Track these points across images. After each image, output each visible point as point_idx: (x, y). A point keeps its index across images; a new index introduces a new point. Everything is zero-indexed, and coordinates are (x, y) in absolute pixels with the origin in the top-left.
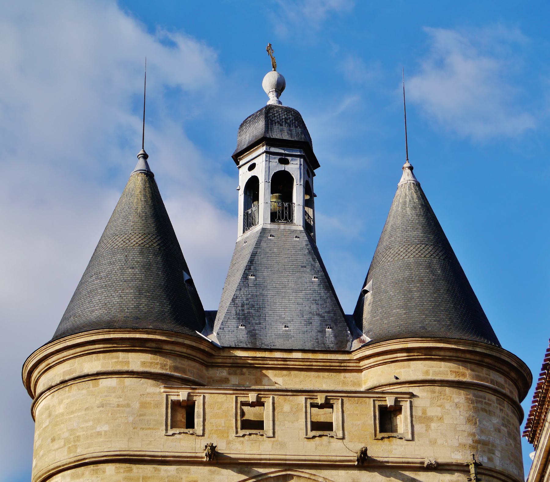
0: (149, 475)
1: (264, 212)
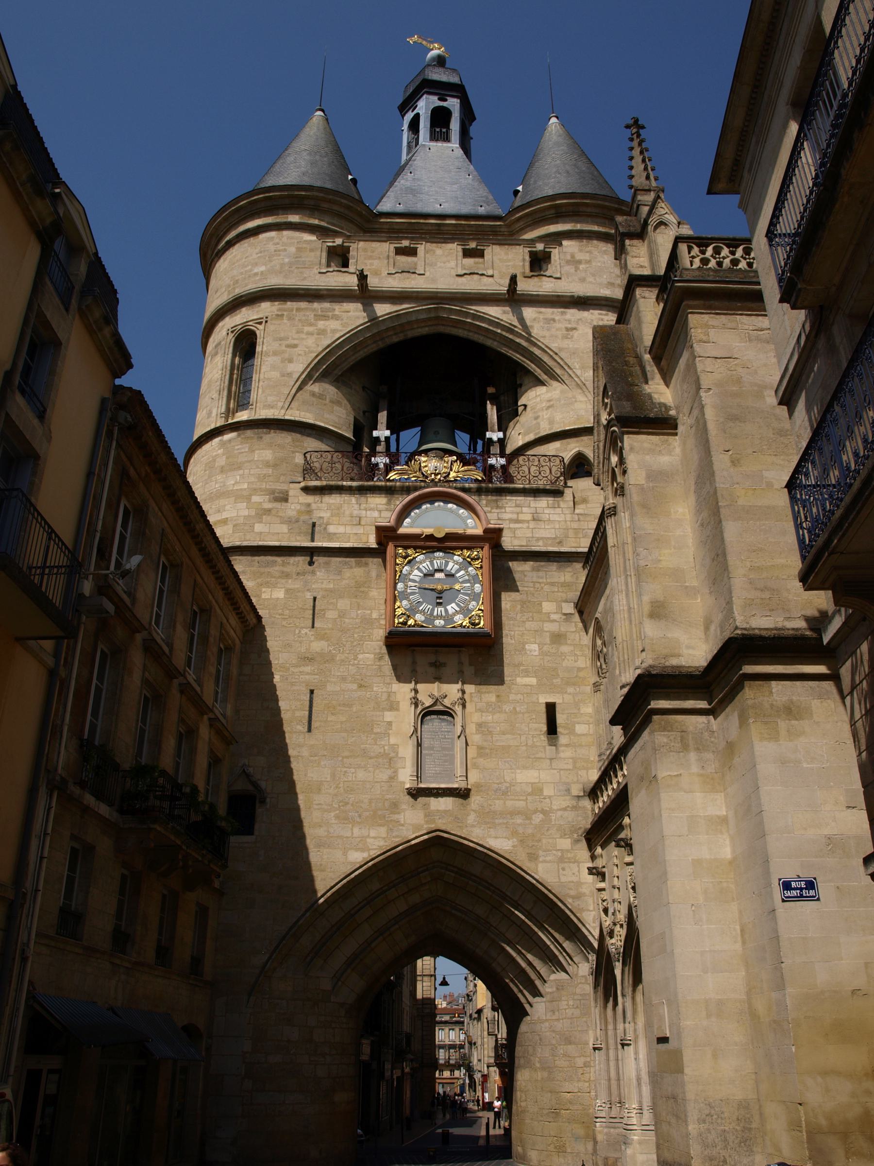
1: (425, 134)
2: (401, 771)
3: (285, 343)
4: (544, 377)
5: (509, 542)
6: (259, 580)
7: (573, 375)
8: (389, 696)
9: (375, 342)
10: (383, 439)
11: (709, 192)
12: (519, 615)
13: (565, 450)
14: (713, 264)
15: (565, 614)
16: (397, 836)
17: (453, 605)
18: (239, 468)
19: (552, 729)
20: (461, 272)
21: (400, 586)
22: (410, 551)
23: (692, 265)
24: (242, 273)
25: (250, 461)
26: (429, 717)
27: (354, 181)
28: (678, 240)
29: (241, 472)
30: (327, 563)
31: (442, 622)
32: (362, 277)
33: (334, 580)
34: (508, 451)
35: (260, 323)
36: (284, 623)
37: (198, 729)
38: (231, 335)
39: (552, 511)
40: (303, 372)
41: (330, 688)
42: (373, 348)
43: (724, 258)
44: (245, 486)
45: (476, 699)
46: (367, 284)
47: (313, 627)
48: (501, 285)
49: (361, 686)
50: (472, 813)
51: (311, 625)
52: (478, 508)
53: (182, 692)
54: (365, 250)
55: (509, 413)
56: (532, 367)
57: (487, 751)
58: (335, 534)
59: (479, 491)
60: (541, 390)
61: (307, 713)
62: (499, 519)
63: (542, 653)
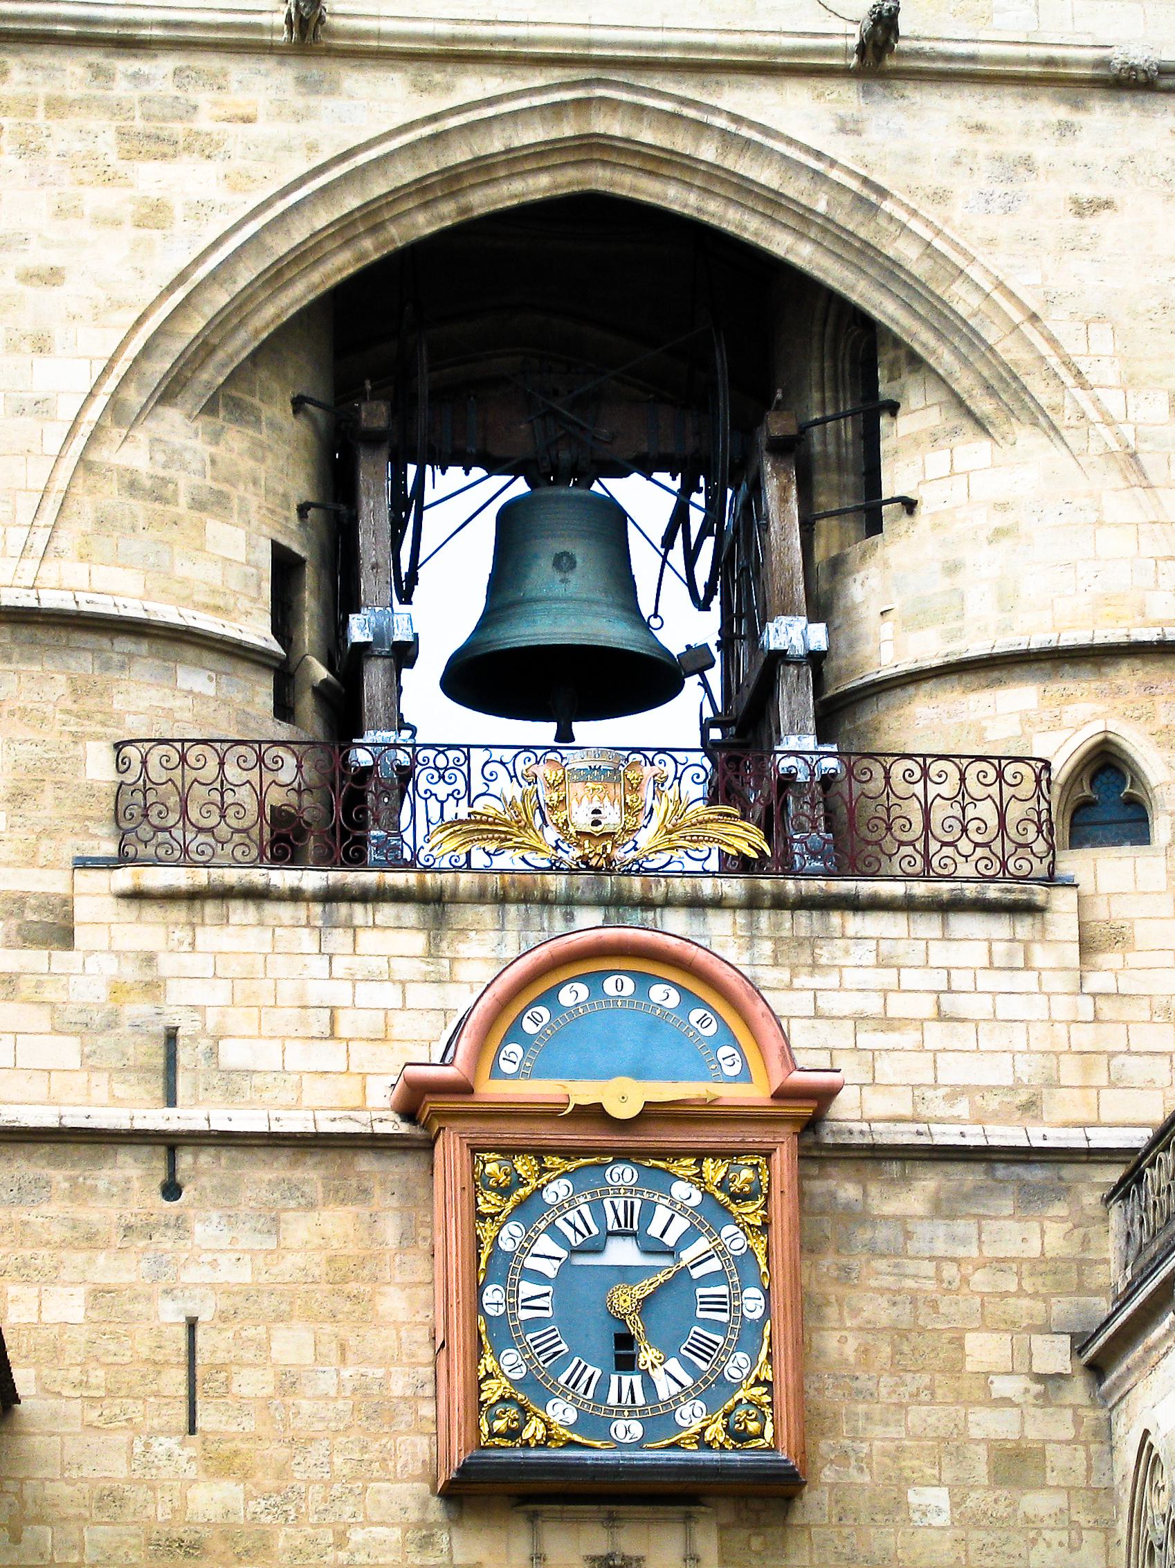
0: (71, 94)
4: (983, 405)
9: (347, 243)
12: (886, 1380)
15: (1040, 1378)
21: (493, 1296)
22: (523, 1165)
31: (637, 1430)
33: (251, 1251)
36: (93, 1415)
39: (1001, 981)
40: (91, 394)
42: (340, 265)
46: (321, 20)
47: (192, 1430)
56: (943, 358)
59: (752, 903)
63: (966, 1520)
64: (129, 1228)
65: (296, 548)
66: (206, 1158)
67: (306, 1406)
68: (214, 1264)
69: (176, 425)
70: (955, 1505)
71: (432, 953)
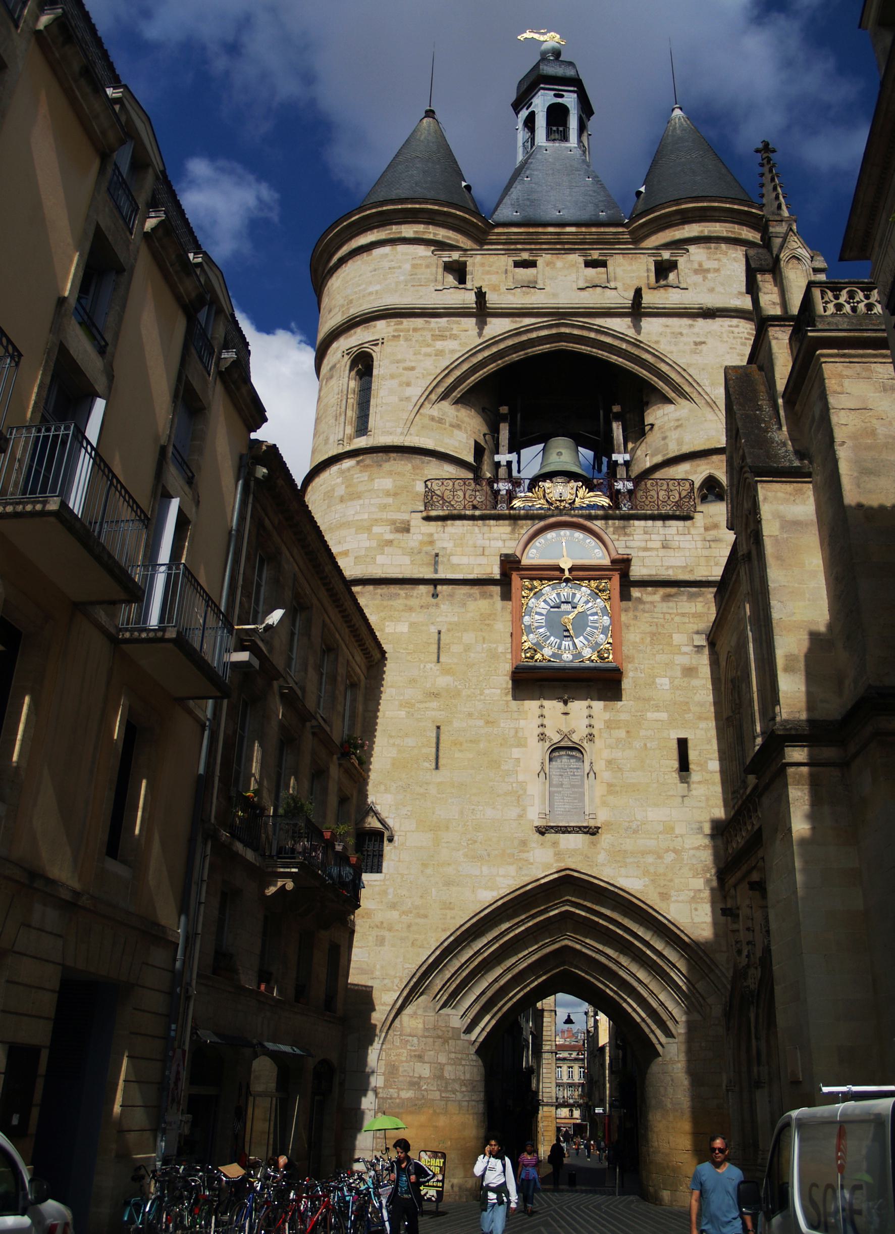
0: (419, 327)
2: (529, 809)
3: (402, 365)
4: (672, 395)
5: (637, 571)
6: (382, 614)
7: (702, 393)
8: (516, 732)
10: (504, 463)
11: (841, 259)
12: (649, 647)
13: (695, 472)
14: (847, 308)
16: (526, 875)
17: (581, 638)
18: (359, 498)
19: (684, 766)
20: (582, 285)
21: (526, 619)
22: (535, 583)
23: (825, 311)
24: (356, 293)
25: (369, 491)
26: (557, 754)
27: (468, 188)
28: (811, 285)
29: (361, 502)
30: (451, 596)
31: (571, 657)
32: (481, 295)
34: (633, 475)
35: (376, 345)
36: (409, 658)
37: (328, 769)
38: (346, 357)
39: (682, 538)
41: (456, 724)
42: (492, 367)
43: (858, 302)
44: (366, 516)
45: (605, 735)
47: (438, 661)
48: (625, 298)
49: (487, 722)
50: (602, 851)
51: (436, 659)
52: (605, 537)
53: (314, 734)
54: (483, 265)
55: (637, 431)
56: (660, 384)
57: (618, 788)
58: (459, 565)
59: (606, 518)
60: (670, 408)
61: (434, 750)
62: (627, 547)
64: (422, 607)
65: (483, 443)
66: (445, 587)
67: (472, 655)
68: (446, 616)
69: (446, 406)
70: (671, 683)
71: (513, 532)
